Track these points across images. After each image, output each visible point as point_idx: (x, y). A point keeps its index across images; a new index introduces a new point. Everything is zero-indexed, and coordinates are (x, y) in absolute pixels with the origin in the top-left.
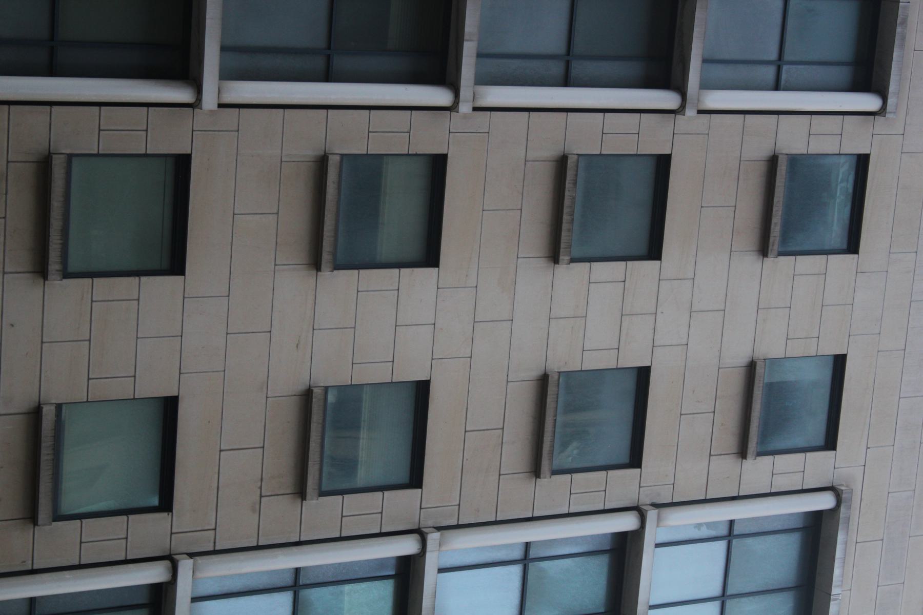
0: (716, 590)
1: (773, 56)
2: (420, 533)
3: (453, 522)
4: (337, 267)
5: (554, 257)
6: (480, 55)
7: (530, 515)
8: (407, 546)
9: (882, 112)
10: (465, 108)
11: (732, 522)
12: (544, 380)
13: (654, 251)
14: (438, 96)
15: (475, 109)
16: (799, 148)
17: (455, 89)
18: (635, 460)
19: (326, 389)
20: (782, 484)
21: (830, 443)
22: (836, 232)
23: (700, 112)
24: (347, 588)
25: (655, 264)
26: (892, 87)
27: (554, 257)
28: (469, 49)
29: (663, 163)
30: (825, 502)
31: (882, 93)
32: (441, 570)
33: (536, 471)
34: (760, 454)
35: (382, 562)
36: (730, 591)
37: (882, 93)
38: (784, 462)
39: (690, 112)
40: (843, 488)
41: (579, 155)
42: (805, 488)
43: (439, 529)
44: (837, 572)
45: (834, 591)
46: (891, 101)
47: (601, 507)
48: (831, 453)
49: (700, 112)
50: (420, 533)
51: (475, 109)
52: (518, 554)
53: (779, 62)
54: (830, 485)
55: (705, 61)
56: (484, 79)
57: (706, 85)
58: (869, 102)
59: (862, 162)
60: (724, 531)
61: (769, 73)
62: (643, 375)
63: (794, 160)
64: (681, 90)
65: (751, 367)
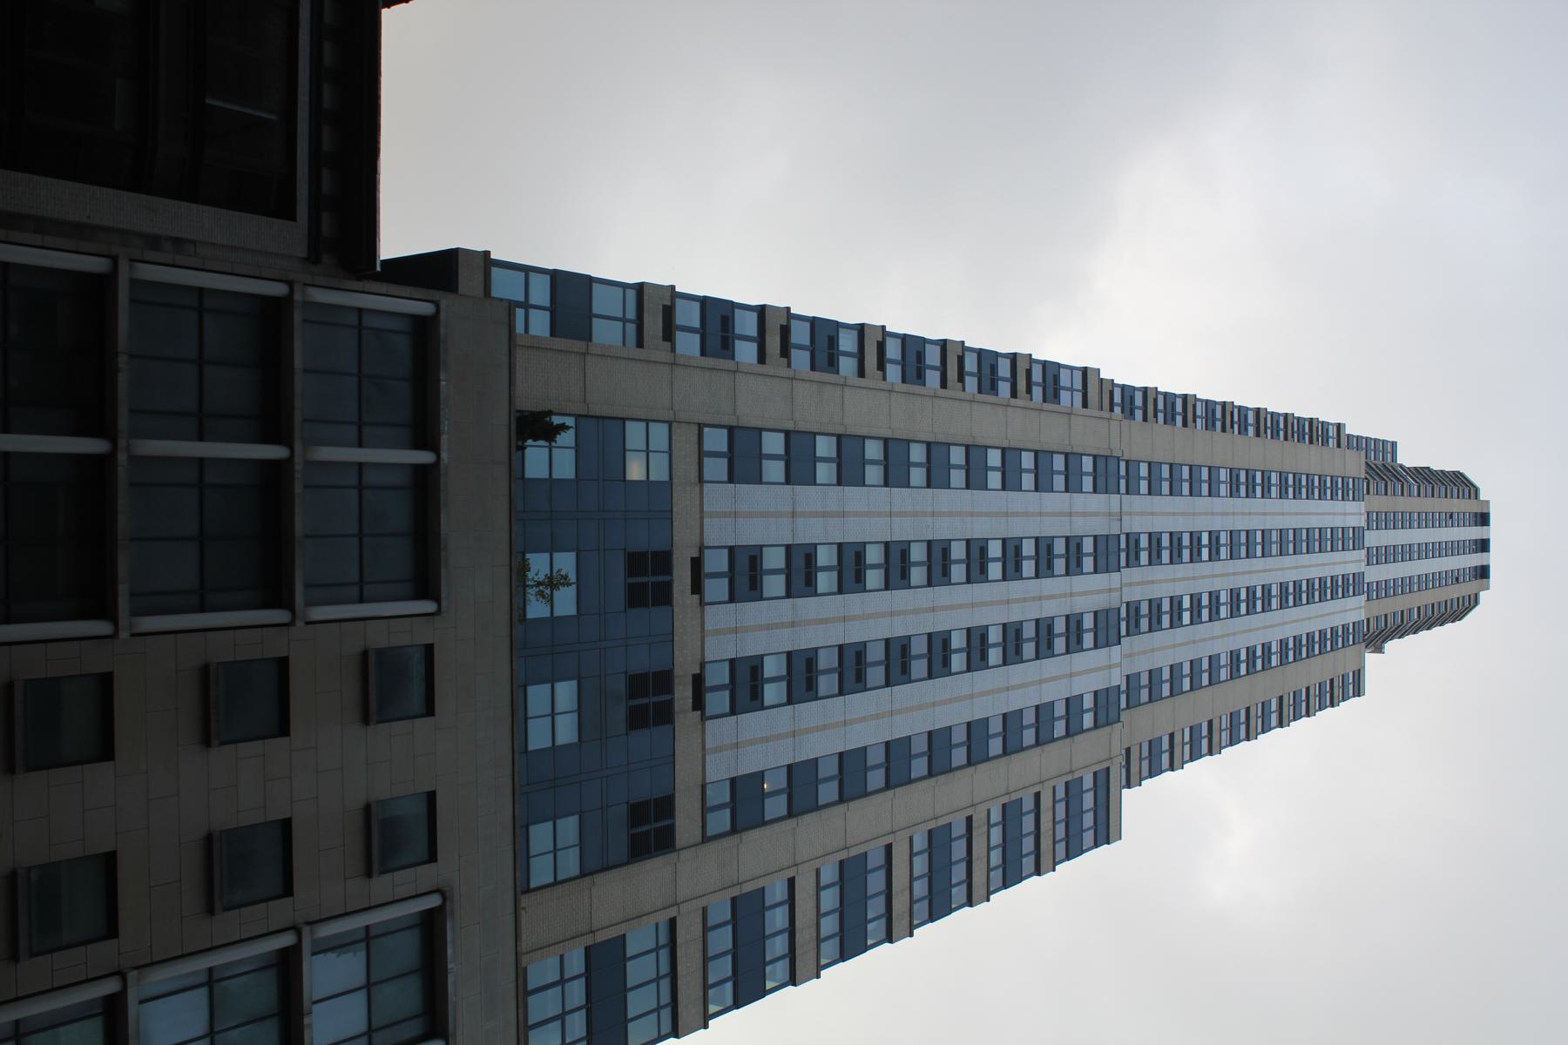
0: (361, 979)
1: (357, 579)
2: (121, 974)
3: (148, 961)
4: (29, 769)
5: (207, 742)
6: (132, 595)
7: (209, 946)
8: (110, 987)
9: (438, 612)
10: (124, 635)
11: (367, 927)
12: (209, 839)
13: (284, 730)
14: (101, 627)
15: (133, 635)
16: (382, 643)
17: (113, 618)
18: (288, 890)
19: (29, 869)
20: (402, 892)
21: (432, 857)
22: (416, 700)
23: (308, 623)
24: (62, 1029)
25: (286, 739)
26: (444, 594)
27: (207, 742)
28: (123, 590)
29: (283, 664)
30: (434, 901)
31: (437, 599)
32: (142, 1002)
33: (211, 911)
34: (383, 872)
35: (89, 1004)
36: (373, 980)
37: (437, 599)
38: (398, 875)
39: (299, 624)
40: (446, 889)
41: (218, 663)
42: (418, 893)
43: (137, 968)
44: (450, 951)
45: (450, 966)
46: (444, 603)
47: (265, 931)
48: (434, 864)
49: (308, 623)
50: (121, 974)
51: (133, 635)
52: (203, 978)
53: (361, 582)
54: (435, 888)
55: (306, 586)
56: (137, 612)
57: (310, 603)
58: (427, 606)
59: (429, 650)
60: (362, 935)
61: (355, 591)
62: (286, 825)
63: (381, 652)
64: (291, 607)
65: (367, 808)
